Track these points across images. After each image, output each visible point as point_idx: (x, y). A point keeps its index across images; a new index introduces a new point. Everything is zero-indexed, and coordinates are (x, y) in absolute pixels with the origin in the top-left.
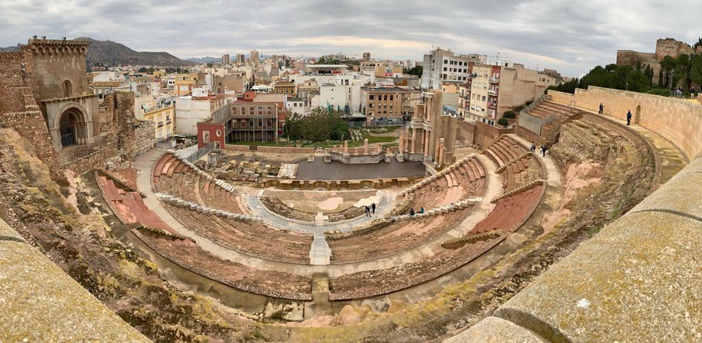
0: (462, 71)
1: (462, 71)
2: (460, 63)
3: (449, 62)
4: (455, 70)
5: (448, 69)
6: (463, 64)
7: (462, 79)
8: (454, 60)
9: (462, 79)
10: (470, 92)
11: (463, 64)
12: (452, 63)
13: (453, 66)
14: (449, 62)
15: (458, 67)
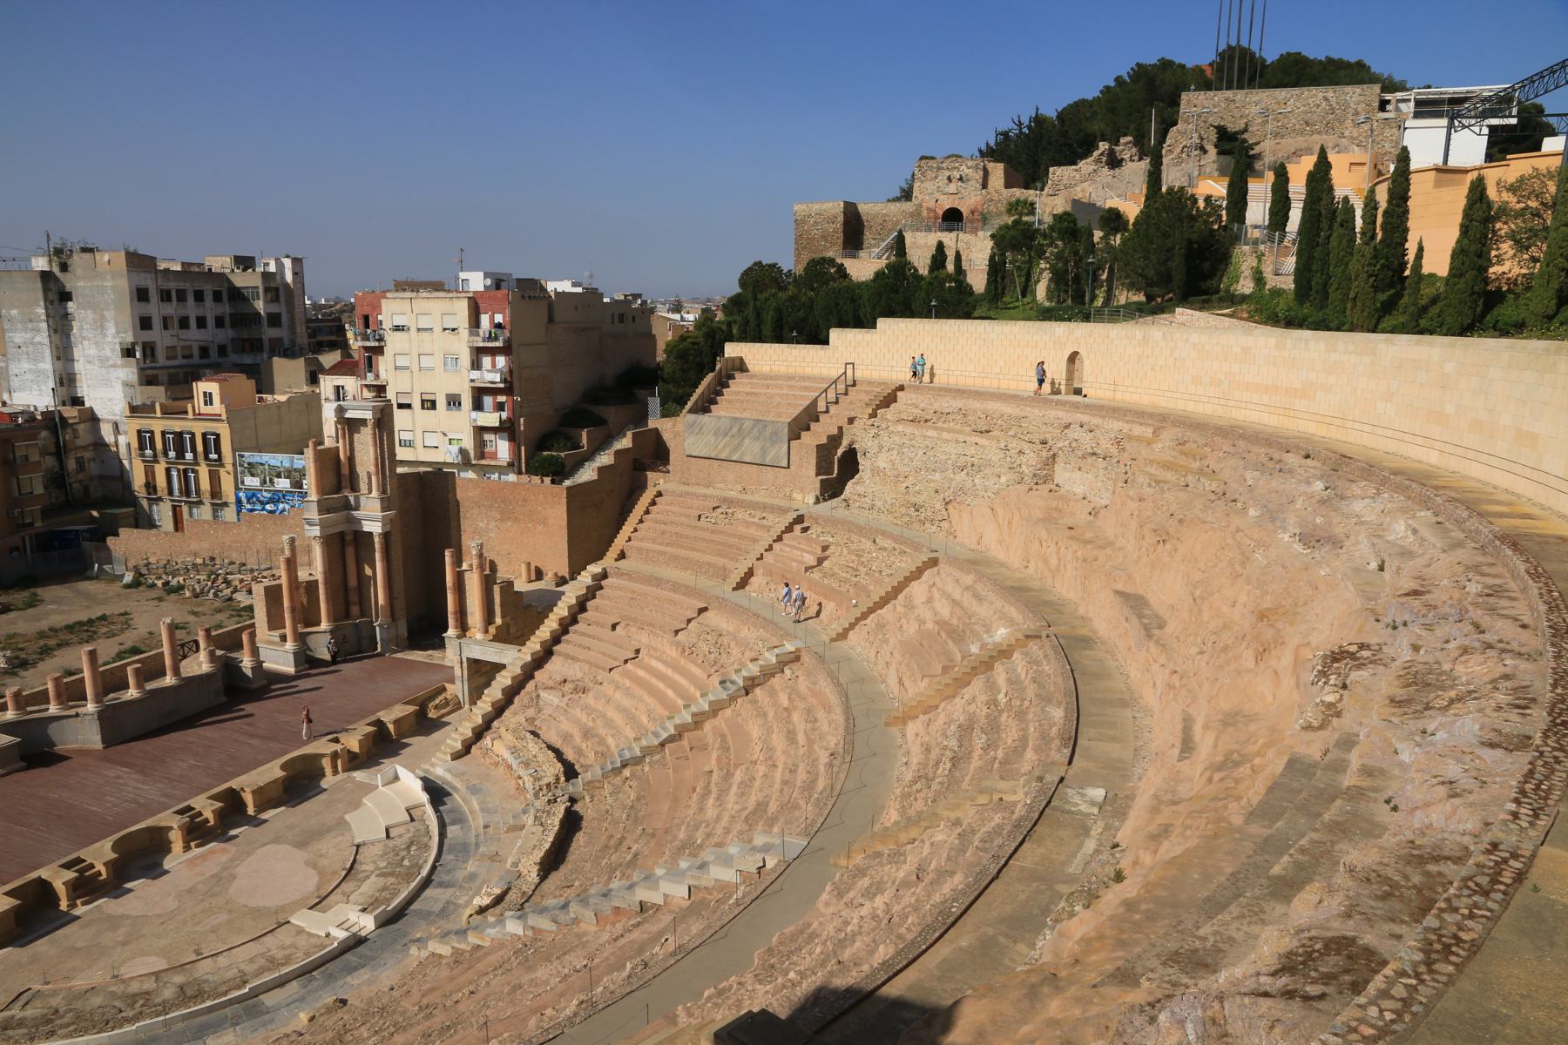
0: (210, 322)
1: (210, 322)
2: (199, 296)
3: (154, 296)
4: (184, 323)
5: (157, 323)
6: (209, 298)
7: (213, 352)
8: (173, 285)
9: (213, 352)
10: (380, 390)
11: (209, 298)
12: (165, 296)
13: (171, 309)
14: (154, 296)
15: (191, 309)
